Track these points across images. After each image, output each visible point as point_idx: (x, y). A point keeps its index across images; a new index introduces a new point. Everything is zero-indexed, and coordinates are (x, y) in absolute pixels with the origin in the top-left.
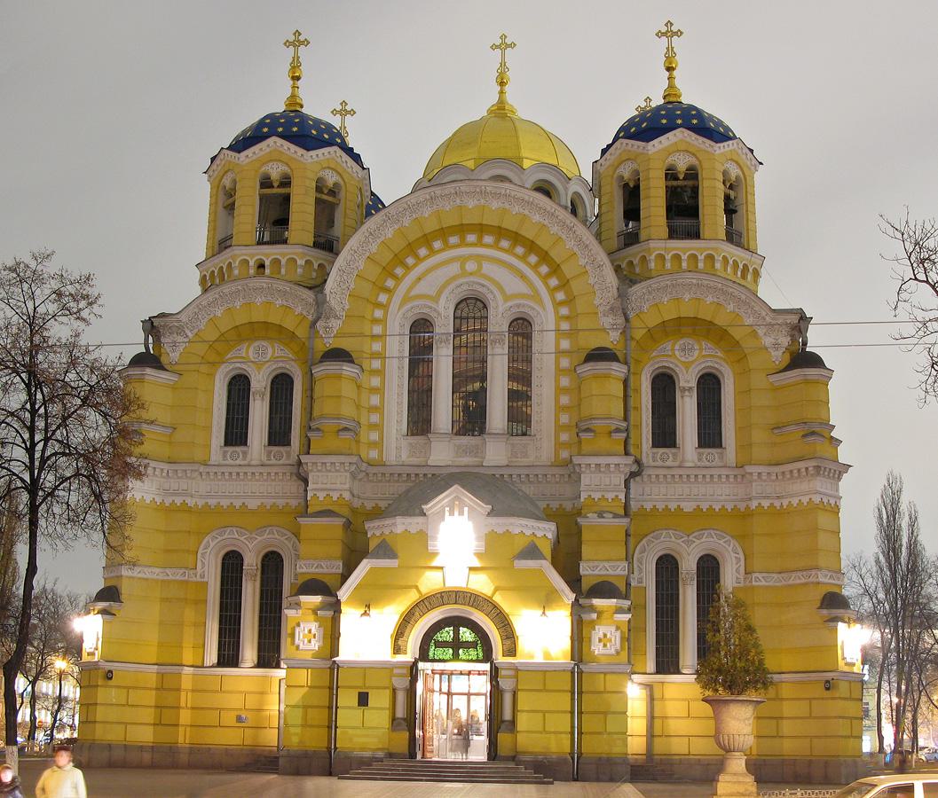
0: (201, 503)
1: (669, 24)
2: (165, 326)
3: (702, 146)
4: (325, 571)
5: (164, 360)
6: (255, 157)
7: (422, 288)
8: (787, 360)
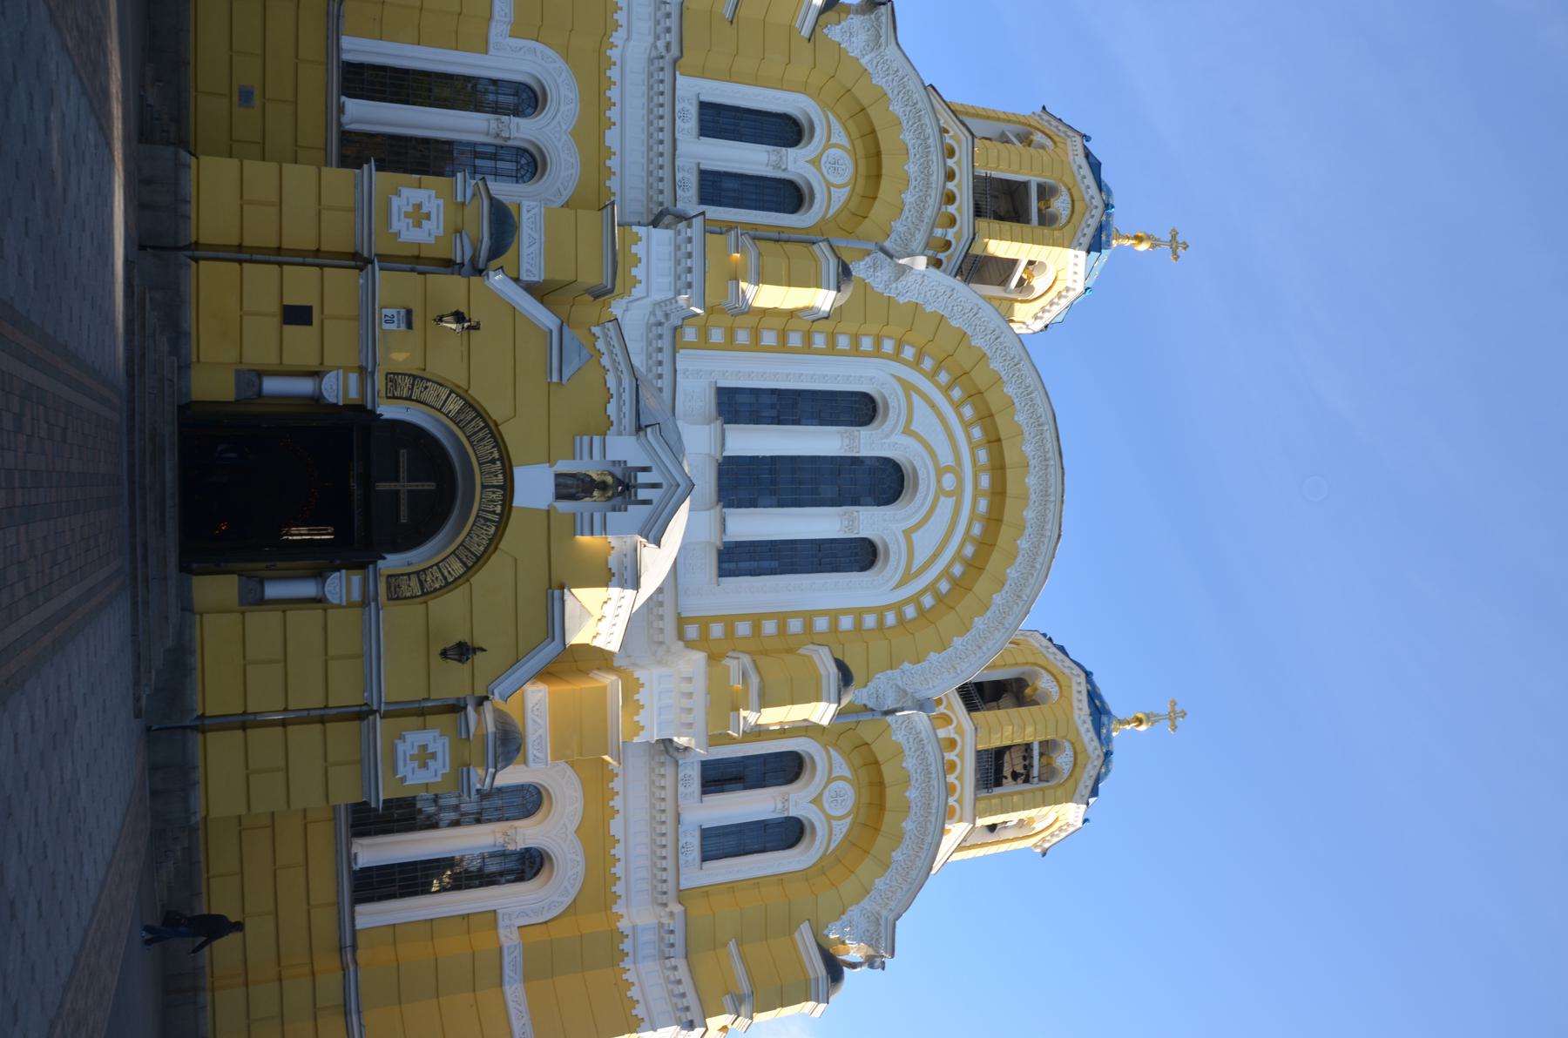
0: (614, 54)
1: (1184, 714)
2: (878, 19)
3: (1081, 786)
4: (525, 251)
5: (831, 15)
6: (1079, 178)
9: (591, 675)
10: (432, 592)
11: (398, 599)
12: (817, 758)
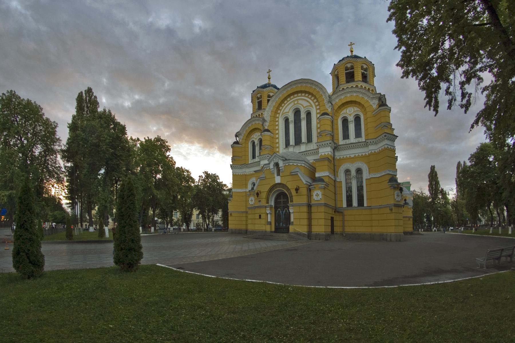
7: (286, 111)
8: (378, 106)
12: (342, 117)
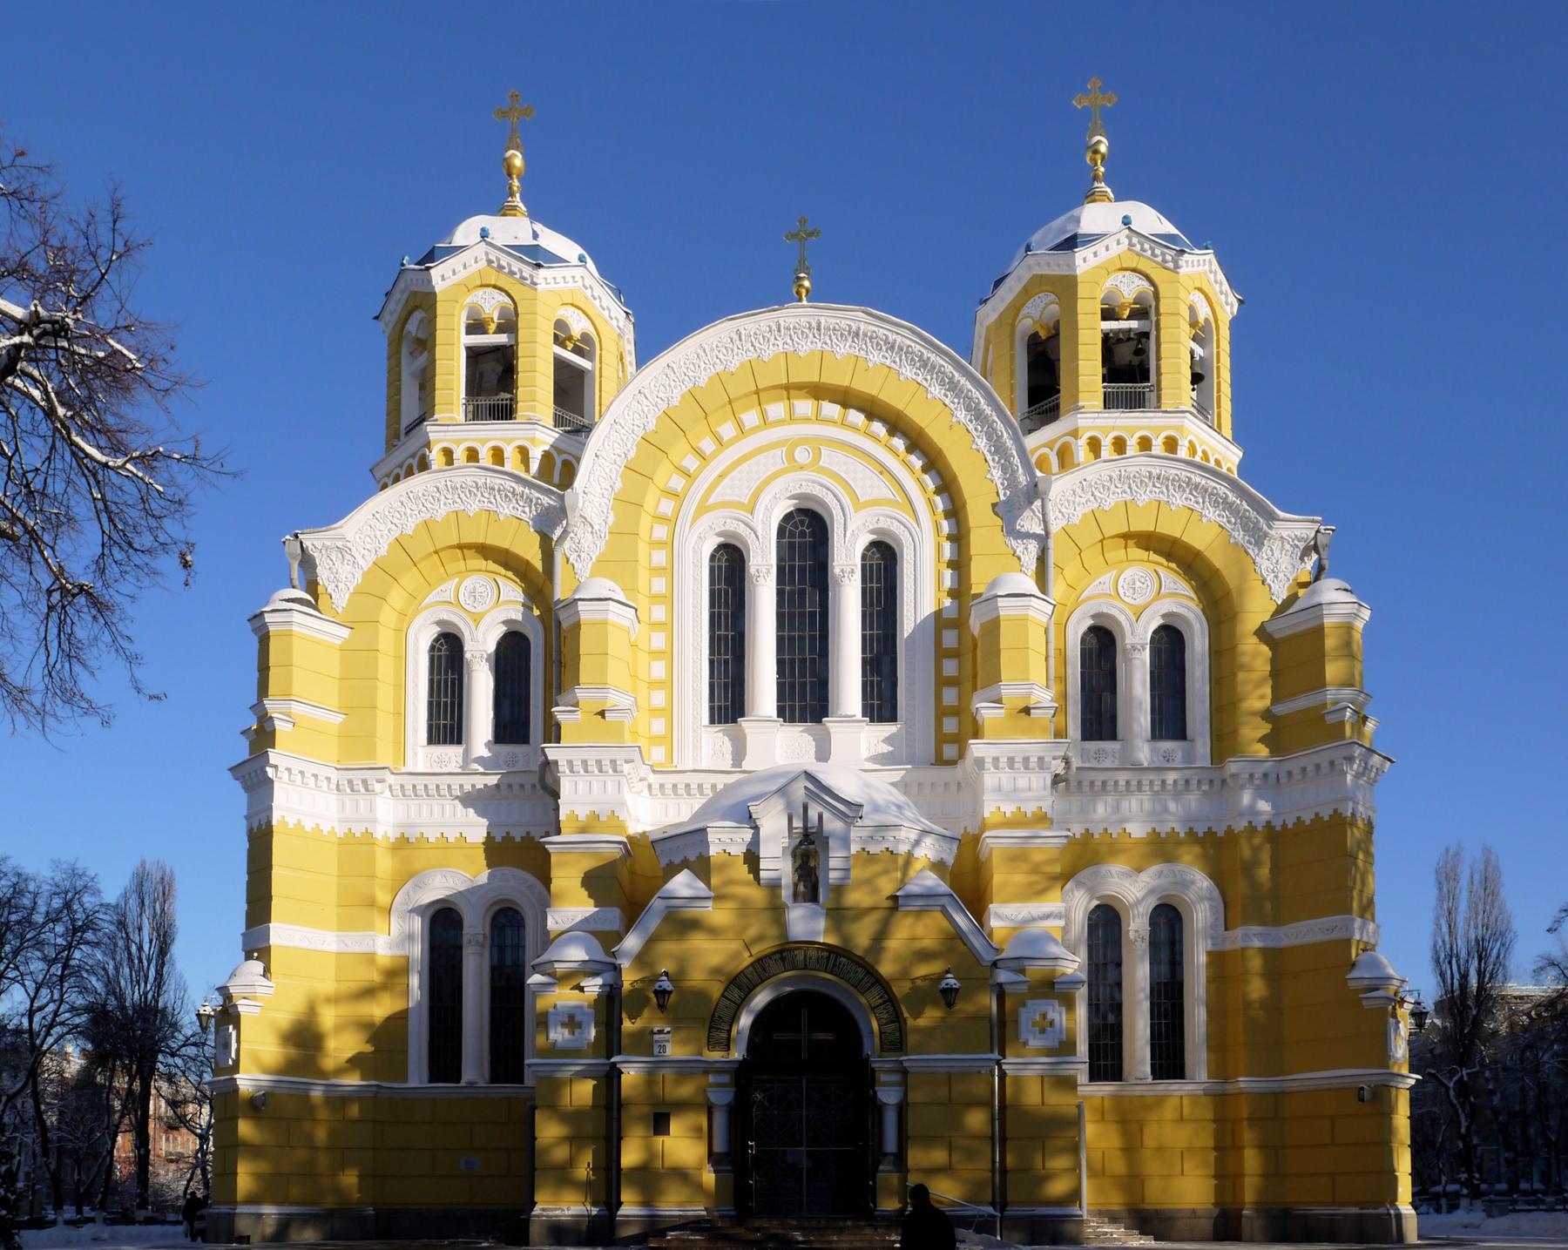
9: (984, 860)
10: (897, 1014)
11: (901, 1043)
